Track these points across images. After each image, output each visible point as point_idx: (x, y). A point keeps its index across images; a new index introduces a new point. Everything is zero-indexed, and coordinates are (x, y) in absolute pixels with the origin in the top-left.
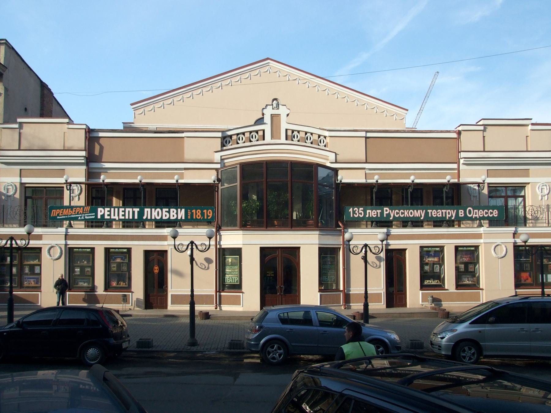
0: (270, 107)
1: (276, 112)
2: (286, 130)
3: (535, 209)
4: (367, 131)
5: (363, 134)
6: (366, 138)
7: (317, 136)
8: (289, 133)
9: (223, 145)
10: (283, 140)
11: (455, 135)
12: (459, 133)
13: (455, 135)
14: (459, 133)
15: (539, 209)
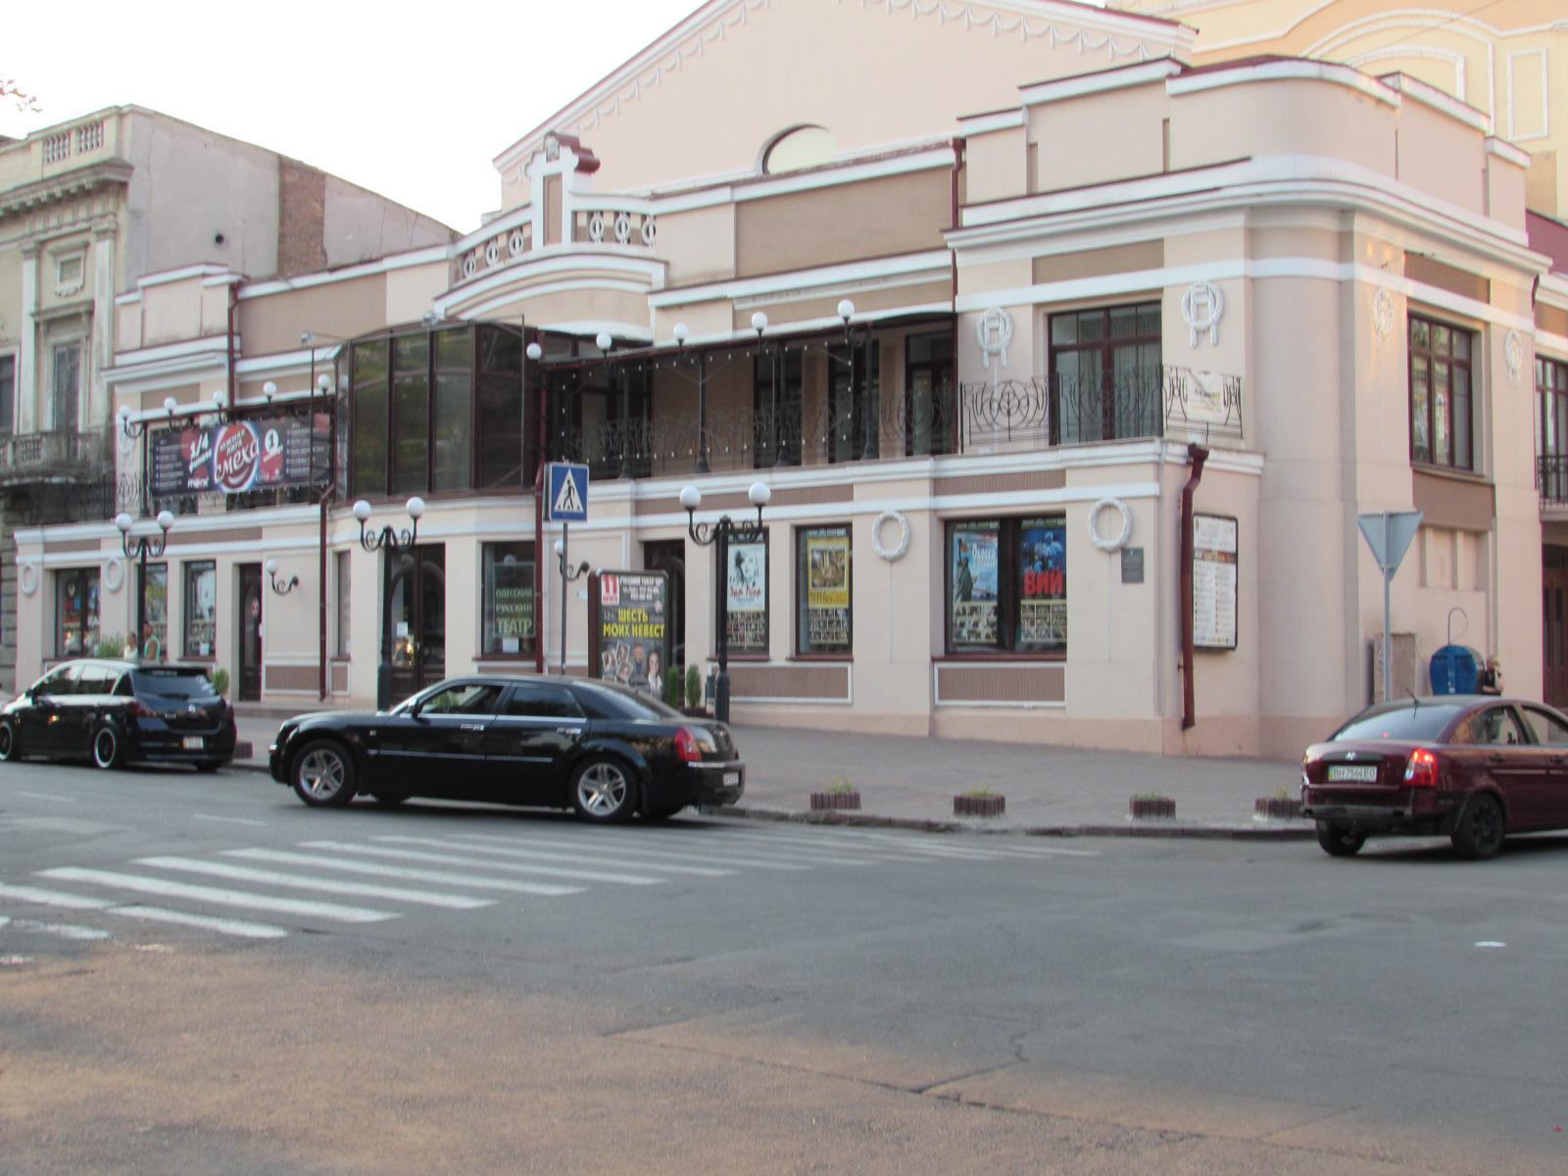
0: (541, 158)
1: (553, 168)
2: (575, 214)
3: (1020, 393)
4: (733, 185)
5: (725, 195)
6: (739, 204)
7: (639, 219)
8: (582, 220)
9: (457, 275)
10: (566, 244)
11: (949, 157)
12: (960, 145)
13: (949, 157)
14: (960, 145)
15: (1031, 391)
